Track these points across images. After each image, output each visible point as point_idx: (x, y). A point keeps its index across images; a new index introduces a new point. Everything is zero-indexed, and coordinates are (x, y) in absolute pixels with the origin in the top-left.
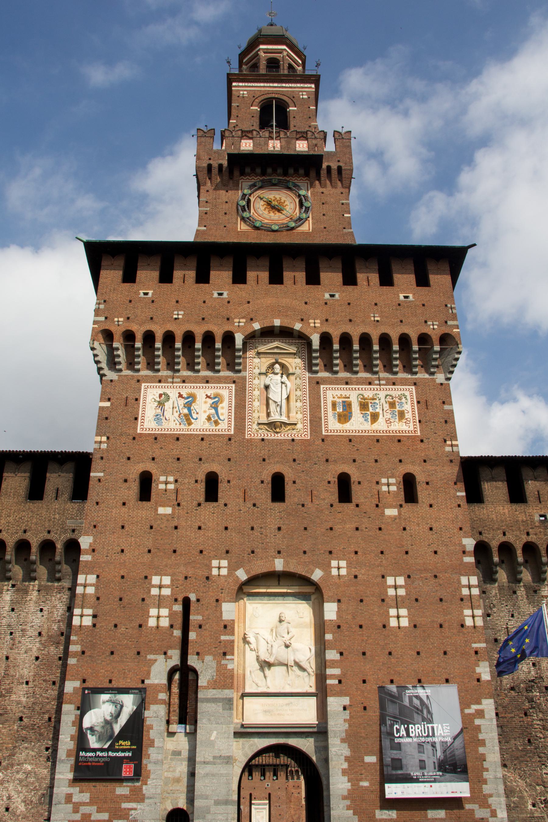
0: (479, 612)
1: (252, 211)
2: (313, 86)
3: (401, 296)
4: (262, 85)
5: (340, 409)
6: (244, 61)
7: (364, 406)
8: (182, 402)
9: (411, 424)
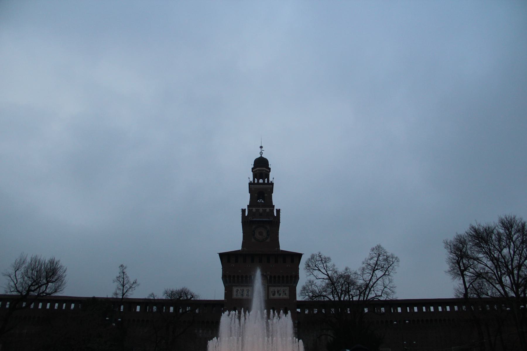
0: (297, 335)
1: (255, 235)
2: (272, 186)
3: (287, 265)
4: (258, 186)
5: (273, 293)
6: (253, 171)
7: (278, 292)
8: (241, 291)
9: (287, 296)
